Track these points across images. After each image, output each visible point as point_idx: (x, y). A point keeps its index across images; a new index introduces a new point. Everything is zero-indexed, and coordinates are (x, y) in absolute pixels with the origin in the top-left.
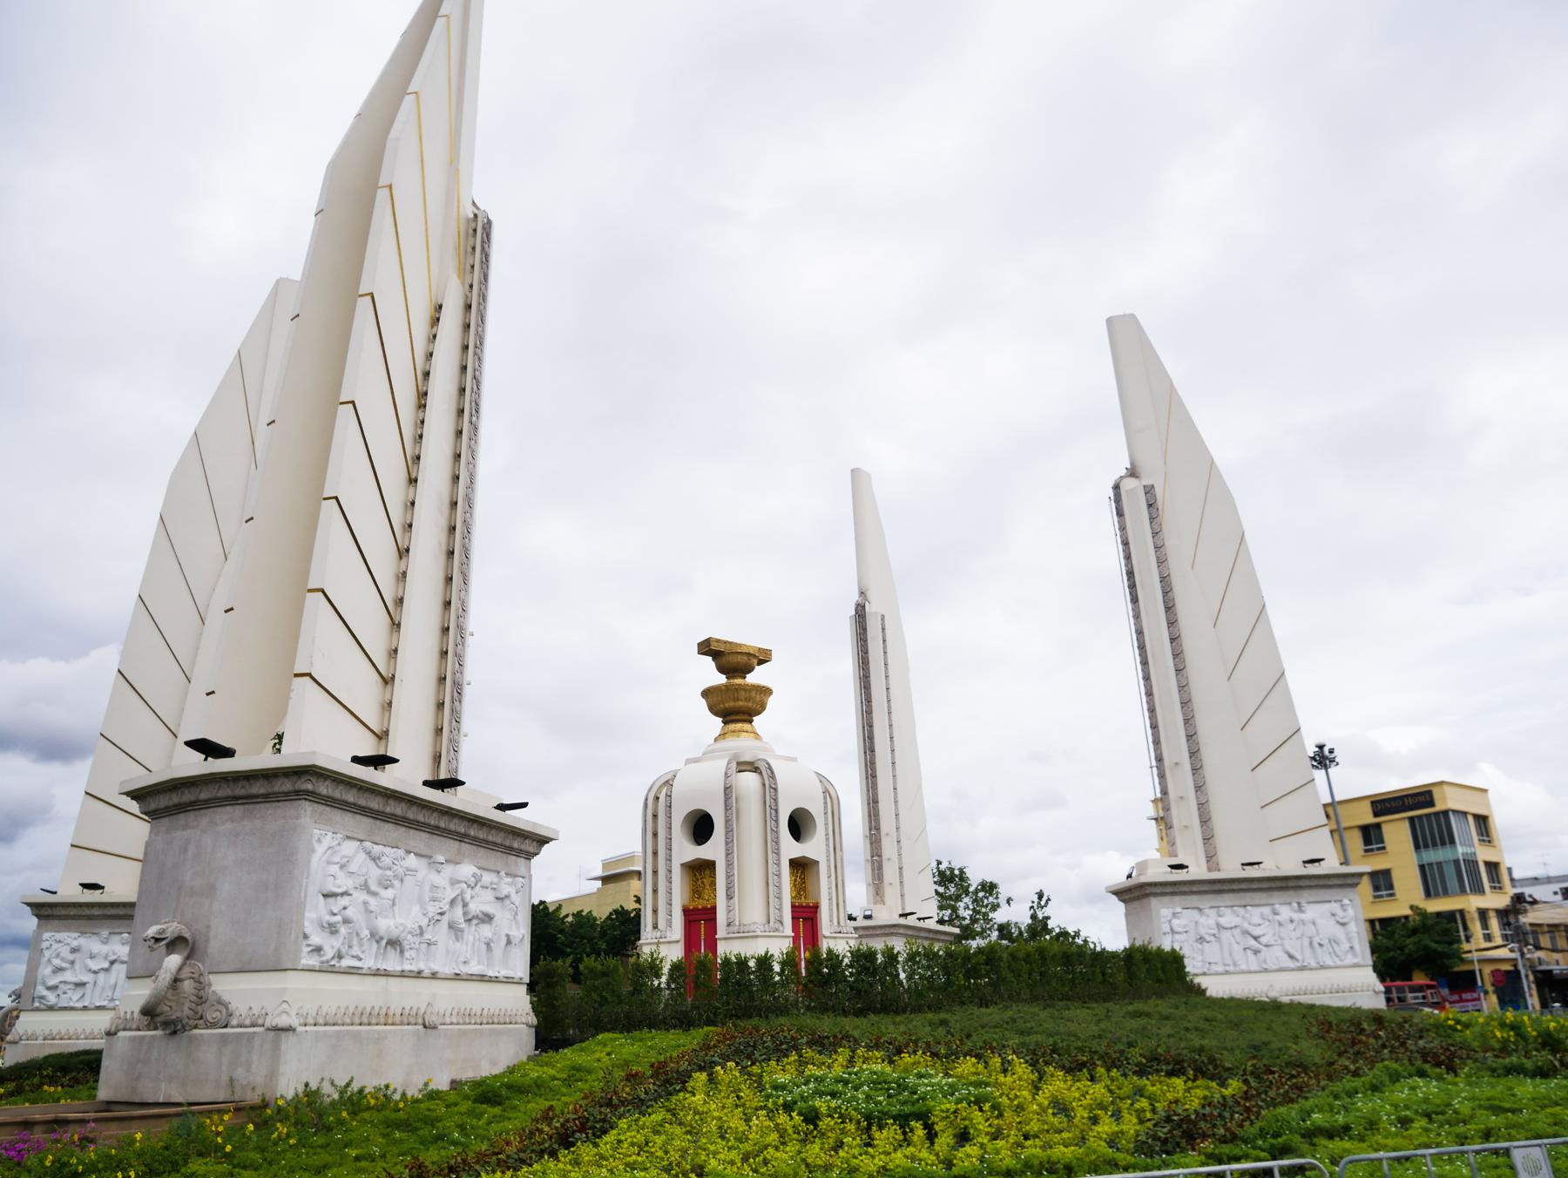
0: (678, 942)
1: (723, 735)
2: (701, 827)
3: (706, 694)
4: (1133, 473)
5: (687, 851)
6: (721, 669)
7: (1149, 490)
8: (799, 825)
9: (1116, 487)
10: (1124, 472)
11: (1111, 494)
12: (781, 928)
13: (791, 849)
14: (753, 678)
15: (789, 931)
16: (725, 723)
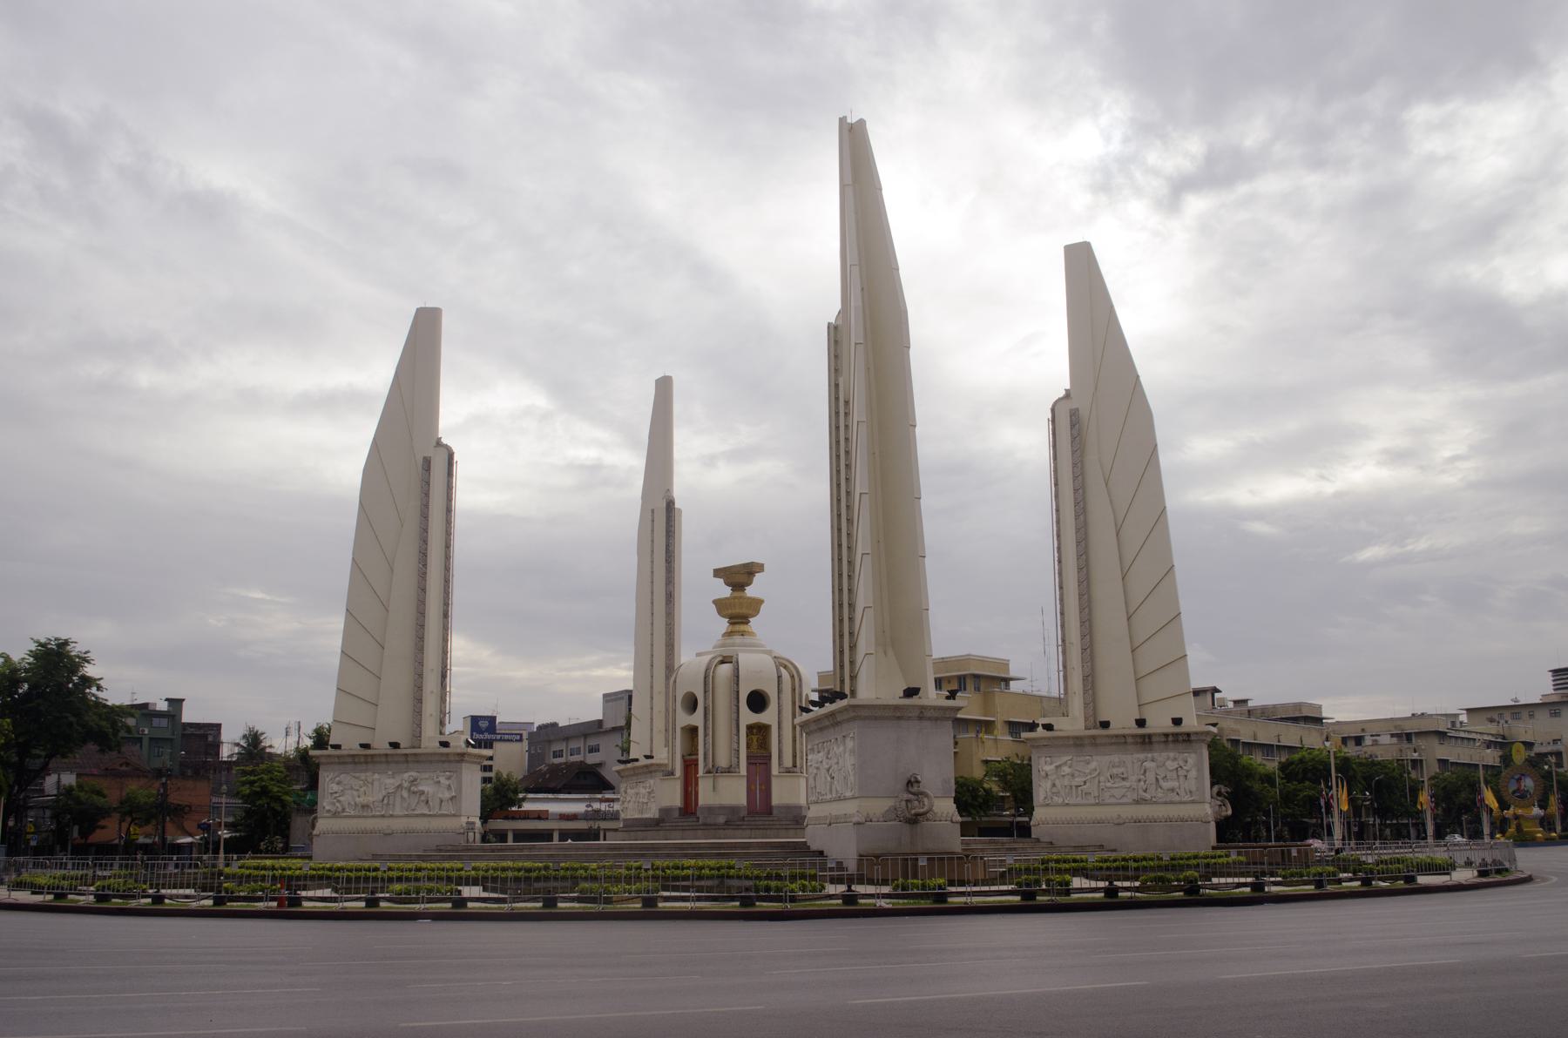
0: (679, 778)
1: (729, 634)
2: (691, 704)
3: (715, 602)
4: (1068, 395)
5: (684, 719)
6: (727, 584)
7: (1074, 414)
8: (758, 701)
9: (1053, 410)
10: (1062, 394)
11: (1050, 416)
12: (737, 770)
13: (748, 717)
14: (750, 591)
15: (743, 770)
16: (731, 624)
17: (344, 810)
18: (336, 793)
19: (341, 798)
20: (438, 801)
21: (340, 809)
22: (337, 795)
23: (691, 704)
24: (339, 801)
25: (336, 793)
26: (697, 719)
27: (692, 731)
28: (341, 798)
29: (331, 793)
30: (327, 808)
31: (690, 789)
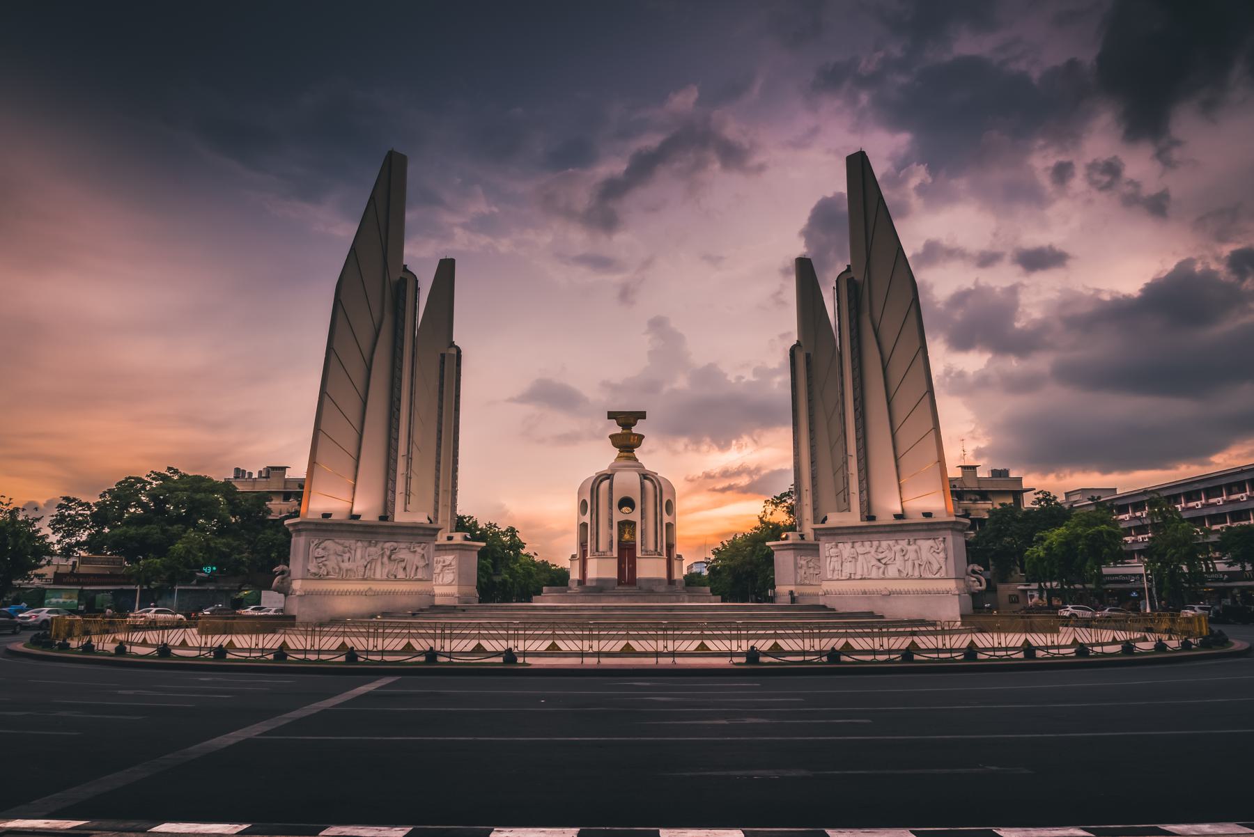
5: (618, 516)
17: (327, 574)
18: (323, 557)
19: (326, 562)
20: (414, 567)
21: (325, 573)
22: (324, 559)
23: (627, 502)
24: (325, 565)
25: (323, 557)
26: (635, 516)
27: (626, 526)
28: (326, 562)
29: (316, 558)
30: (313, 571)
31: (623, 566)
